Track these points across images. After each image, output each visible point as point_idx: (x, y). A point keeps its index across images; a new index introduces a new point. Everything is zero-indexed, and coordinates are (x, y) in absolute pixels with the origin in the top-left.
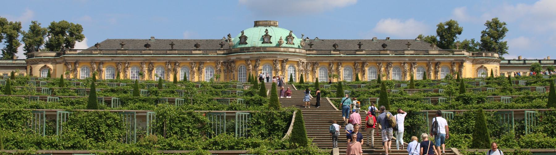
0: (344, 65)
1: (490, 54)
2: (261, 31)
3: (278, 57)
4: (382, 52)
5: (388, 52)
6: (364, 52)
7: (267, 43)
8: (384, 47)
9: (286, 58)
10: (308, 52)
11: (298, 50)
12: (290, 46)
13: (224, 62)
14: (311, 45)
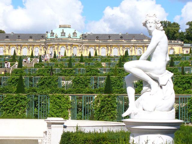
0: (101, 47)
1: (176, 42)
2: (61, 30)
4: (120, 40)
5: (123, 40)
6: (111, 40)
7: (63, 36)
8: (121, 38)
9: (72, 43)
10: (84, 40)
11: (78, 40)
12: (75, 37)
13: (44, 46)
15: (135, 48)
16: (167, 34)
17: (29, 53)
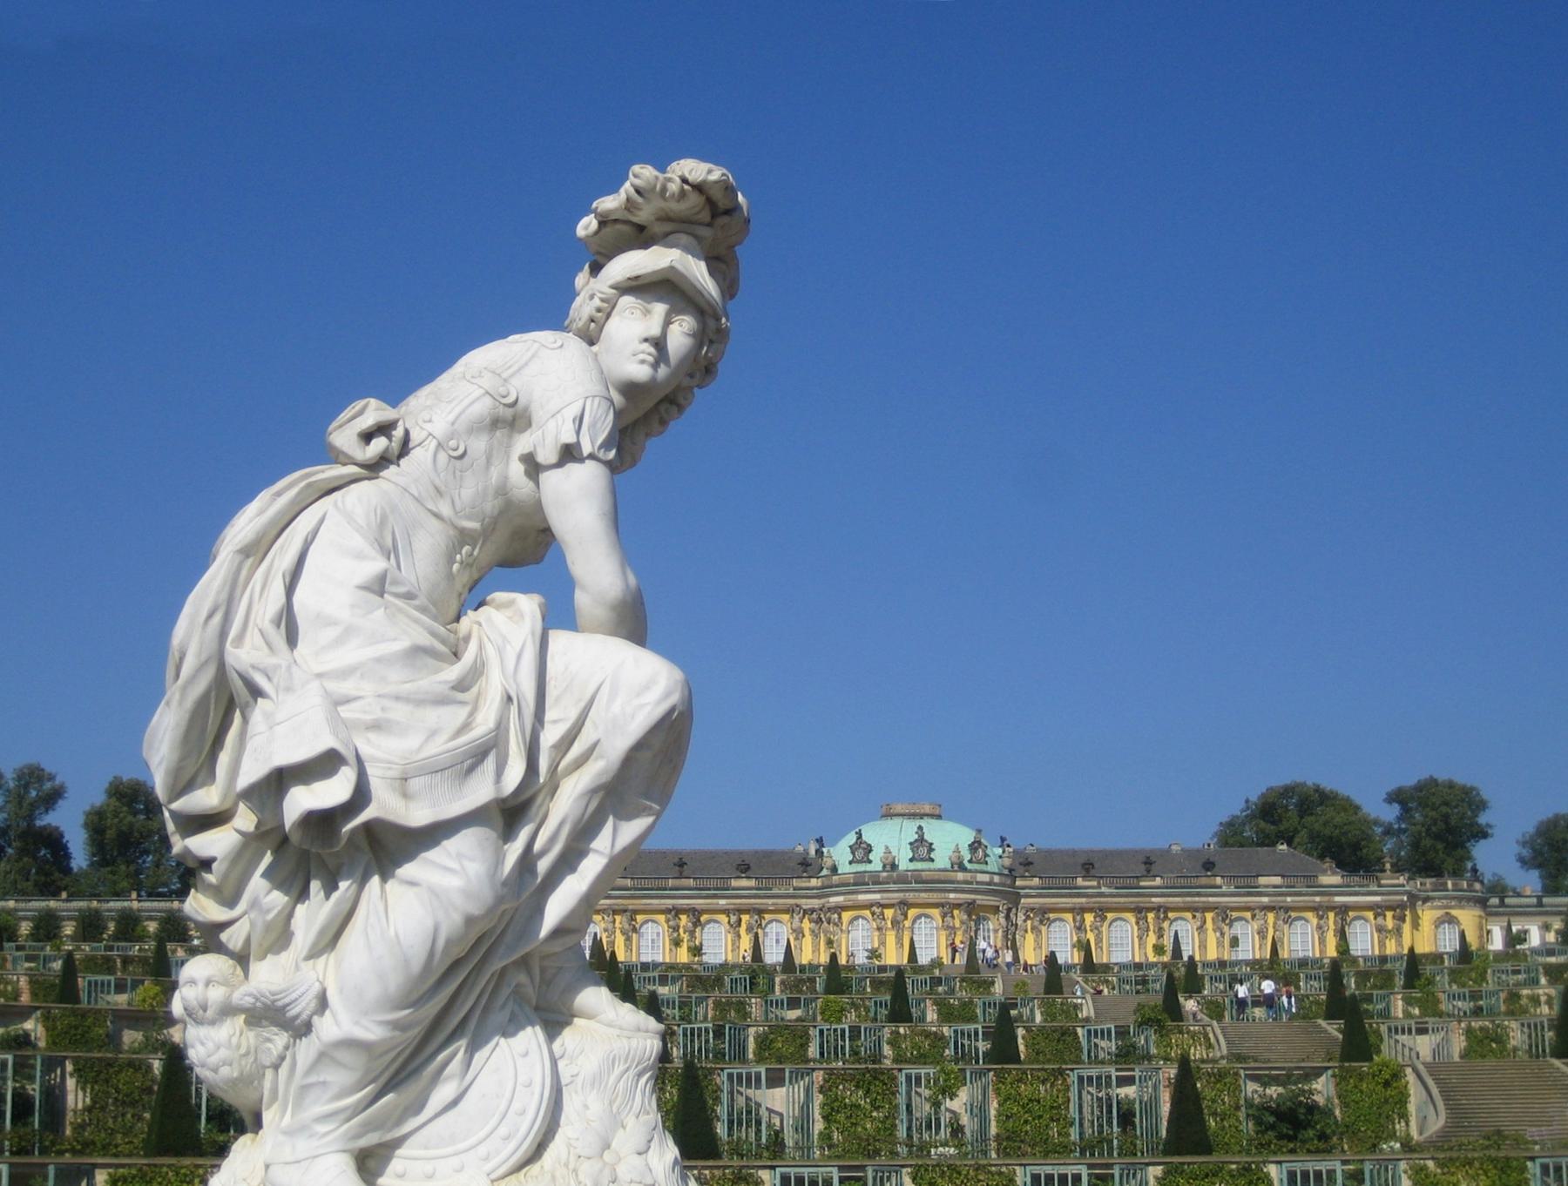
3: (952, 895)
4: (1204, 881)
5: (1219, 880)
6: (1158, 881)
7: (922, 860)
11: (996, 879)
13: (813, 911)
14: (1027, 864)
15: (1277, 918)
16: (1460, 851)
17: (736, 948)
